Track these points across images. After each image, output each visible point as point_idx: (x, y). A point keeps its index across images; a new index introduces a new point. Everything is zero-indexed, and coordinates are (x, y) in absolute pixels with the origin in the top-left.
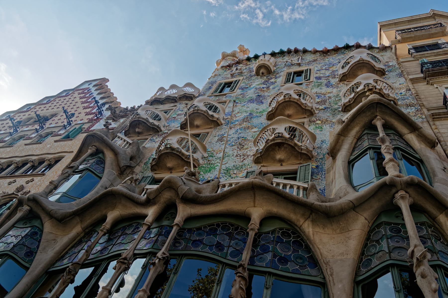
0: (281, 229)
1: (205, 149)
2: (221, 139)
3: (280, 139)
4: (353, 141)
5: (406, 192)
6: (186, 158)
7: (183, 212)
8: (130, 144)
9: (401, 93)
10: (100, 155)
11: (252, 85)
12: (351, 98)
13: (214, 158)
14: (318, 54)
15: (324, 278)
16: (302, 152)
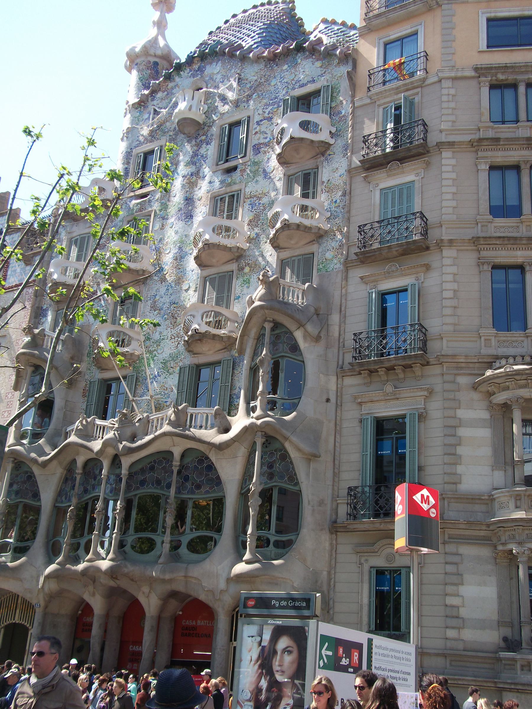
9: (336, 202)
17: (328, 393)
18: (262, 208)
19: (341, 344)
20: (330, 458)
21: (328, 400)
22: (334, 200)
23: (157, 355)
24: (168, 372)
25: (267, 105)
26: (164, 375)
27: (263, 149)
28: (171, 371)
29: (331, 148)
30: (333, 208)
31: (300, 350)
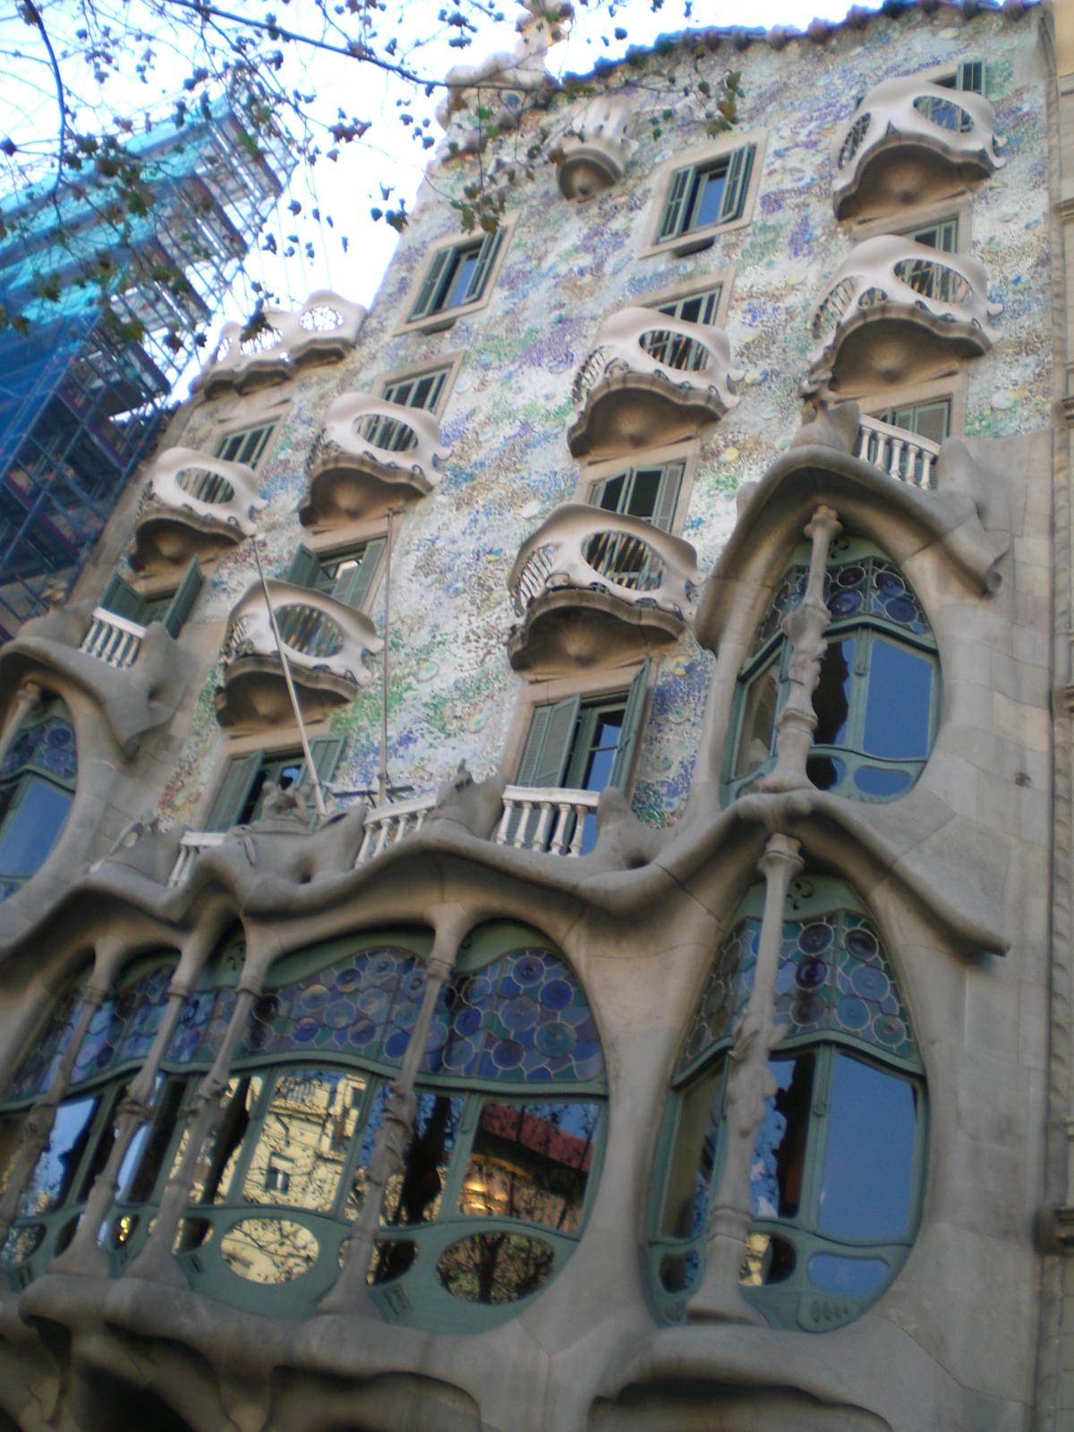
0: (518, 953)
1: (367, 625)
2: (424, 567)
3: (564, 597)
4: (756, 600)
5: (790, 835)
6: (309, 678)
7: (261, 945)
8: (140, 641)
9: (1017, 281)
10: (56, 710)
11: (546, 252)
12: (828, 348)
13: (403, 651)
14: (793, 49)
15: (606, 1084)
16: (645, 622)
17: (1021, 757)
18: (784, 317)
19: (1060, 622)
20: (1034, 970)
21: (1022, 780)
22: (1012, 277)
23: (415, 685)
24: (442, 729)
25: (803, 122)
26: (429, 739)
27: (789, 201)
28: (453, 726)
29: (996, 175)
30: (1010, 296)
31: (923, 618)
